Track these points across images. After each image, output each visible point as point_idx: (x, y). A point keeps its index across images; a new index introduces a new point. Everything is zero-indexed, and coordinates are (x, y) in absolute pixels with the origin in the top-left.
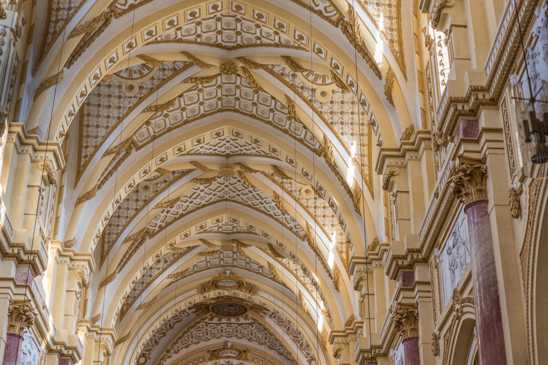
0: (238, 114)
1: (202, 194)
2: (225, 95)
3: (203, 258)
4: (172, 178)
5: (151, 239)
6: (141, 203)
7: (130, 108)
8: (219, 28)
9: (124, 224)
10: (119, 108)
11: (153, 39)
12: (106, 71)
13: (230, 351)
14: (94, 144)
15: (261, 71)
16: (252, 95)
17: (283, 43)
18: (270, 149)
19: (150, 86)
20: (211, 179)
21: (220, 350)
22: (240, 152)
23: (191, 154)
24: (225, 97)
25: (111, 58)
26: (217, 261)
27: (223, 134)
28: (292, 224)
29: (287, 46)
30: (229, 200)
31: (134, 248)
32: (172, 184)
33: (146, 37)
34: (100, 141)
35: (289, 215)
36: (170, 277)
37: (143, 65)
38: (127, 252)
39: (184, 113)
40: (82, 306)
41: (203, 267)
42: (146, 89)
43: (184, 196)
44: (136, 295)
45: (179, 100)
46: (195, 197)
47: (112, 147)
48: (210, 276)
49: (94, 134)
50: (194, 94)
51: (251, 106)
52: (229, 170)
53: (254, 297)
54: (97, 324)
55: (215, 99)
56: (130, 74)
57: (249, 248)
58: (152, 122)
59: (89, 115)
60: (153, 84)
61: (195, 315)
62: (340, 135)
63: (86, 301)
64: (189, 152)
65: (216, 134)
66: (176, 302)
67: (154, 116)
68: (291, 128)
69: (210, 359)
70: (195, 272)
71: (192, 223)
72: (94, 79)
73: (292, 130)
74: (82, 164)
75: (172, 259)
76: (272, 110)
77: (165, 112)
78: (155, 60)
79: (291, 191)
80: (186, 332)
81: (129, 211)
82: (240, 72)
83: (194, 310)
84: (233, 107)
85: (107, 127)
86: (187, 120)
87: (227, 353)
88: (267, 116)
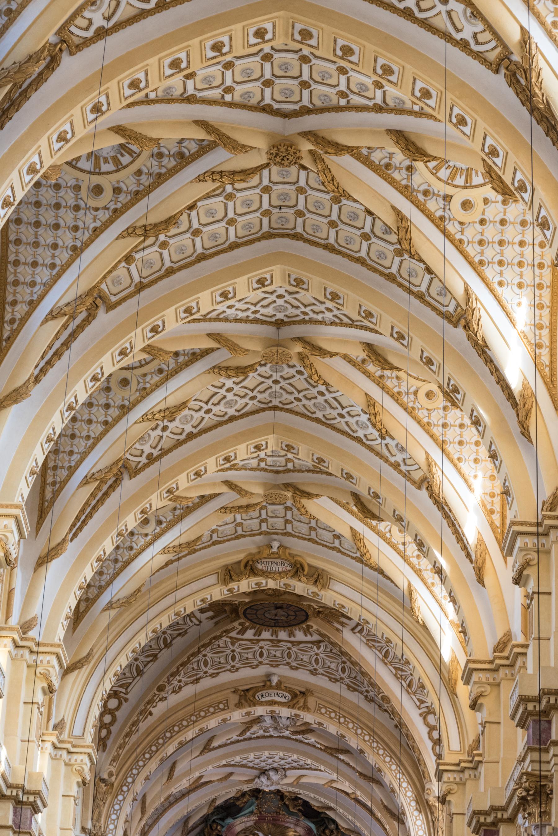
0: (300, 243)
1: (230, 396)
2: (276, 207)
3: (229, 518)
4: (172, 364)
5: (133, 479)
6: (114, 412)
7: (95, 229)
8: (268, 75)
9: (82, 449)
10: (76, 228)
11: (140, 96)
13: (275, 691)
14: (28, 298)
15: (347, 160)
16: (328, 207)
17: (391, 103)
18: (359, 312)
19: (133, 187)
20: (246, 367)
21: (256, 689)
23: (210, 320)
24: (277, 210)
26: (254, 524)
27: (272, 281)
28: (399, 458)
29: (399, 111)
30: (281, 409)
31: (100, 495)
32: (172, 376)
33: (128, 92)
34: (39, 293)
35: (393, 439)
36: (166, 551)
37: (121, 146)
38: (87, 503)
39: (198, 240)
41: (229, 533)
42: (126, 192)
43: (195, 400)
44: (103, 583)
45: (189, 215)
46: (216, 402)
47: (60, 304)
48: (240, 552)
49: (29, 279)
50: (217, 203)
51: (325, 228)
53: (322, 593)
54: (31, 634)
55: (258, 214)
56: (97, 165)
57: (315, 500)
58: (138, 256)
59: (18, 242)
60: (139, 184)
61: (211, 623)
63: (11, 592)
64: (205, 316)
65: (258, 282)
66: (177, 599)
67: (142, 246)
68: (401, 272)
69: (239, 705)
70: (214, 544)
71: (211, 450)
73: (403, 276)
75: (170, 517)
76: (366, 237)
79: (399, 393)
80: (194, 655)
81: (93, 426)
82: (307, 161)
83: (210, 614)
84: (292, 229)
86: (203, 253)
87: (270, 695)
88: (356, 248)
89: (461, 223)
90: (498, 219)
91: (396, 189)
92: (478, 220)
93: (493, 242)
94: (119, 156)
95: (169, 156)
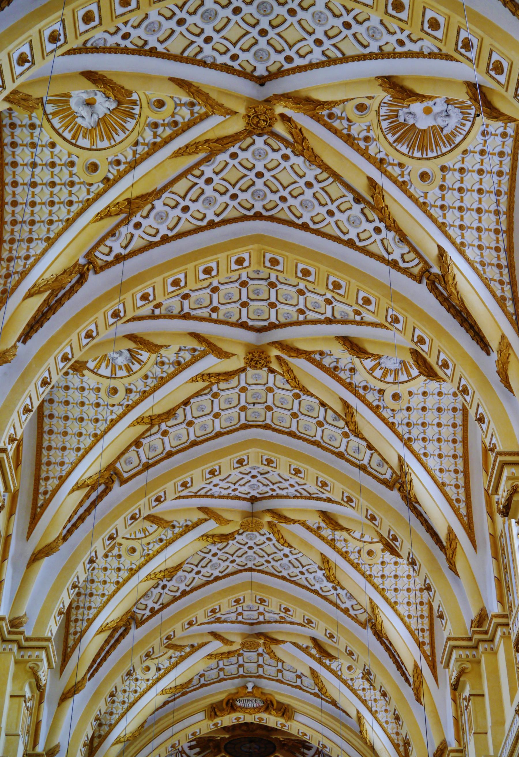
0: (269, 432)
2: (251, 403)
5: (139, 629)
12: (81, 350)
14: (58, 474)
16: (291, 402)
18: (317, 483)
20: (228, 535)
22: (271, 493)
23: (200, 496)
24: (251, 406)
25: (88, 331)
27: (248, 462)
31: (112, 641)
32: (170, 543)
34: (67, 470)
36: (164, 692)
39: (191, 429)
40: (32, 730)
42: (136, 392)
43: (188, 563)
45: (184, 409)
46: (204, 565)
47: (84, 478)
50: (205, 400)
51: (288, 418)
52: (254, 521)
55: (237, 409)
58: (144, 441)
60: (146, 386)
62: (422, 457)
64: (196, 493)
65: (238, 462)
66: (174, 732)
67: (148, 434)
68: (348, 450)
72: (62, 361)
73: (350, 453)
74: (39, 504)
76: (320, 424)
77: (163, 427)
78: (152, 343)
81: (107, 586)
84: (263, 421)
85: (78, 449)
86: (195, 440)
88: (313, 434)
89: (393, 410)
90: (420, 407)
91: (342, 385)
92: (405, 407)
93: (418, 424)
94: (130, 364)
95: (169, 364)
